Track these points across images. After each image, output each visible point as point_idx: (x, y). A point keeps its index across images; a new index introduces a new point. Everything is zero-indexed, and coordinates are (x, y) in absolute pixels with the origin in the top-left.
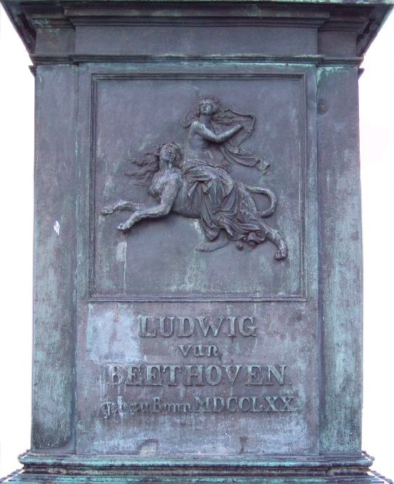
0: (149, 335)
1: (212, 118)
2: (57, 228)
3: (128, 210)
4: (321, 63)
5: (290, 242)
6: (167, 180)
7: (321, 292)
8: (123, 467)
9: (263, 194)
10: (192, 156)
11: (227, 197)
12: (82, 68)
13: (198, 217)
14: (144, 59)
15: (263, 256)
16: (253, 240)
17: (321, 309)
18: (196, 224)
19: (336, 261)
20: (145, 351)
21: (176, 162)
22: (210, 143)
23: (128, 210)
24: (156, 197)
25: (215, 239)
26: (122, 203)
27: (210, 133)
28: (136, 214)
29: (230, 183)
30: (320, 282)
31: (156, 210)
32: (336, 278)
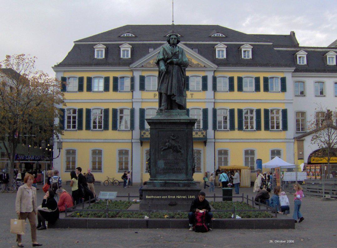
0: (165, 164)
1: (173, 136)
2: (154, 150)
3: (162, 148)
4: (187, 129)
5: (183, 152)
6: (167, 144)
7: (187, 158)
8: (162, 180)
9: (179, 146)
10: (171, 141)
11: (175, 146)
12: (157, 130)
13: (171, 149)
14: (165, 129)
15: (179, 154)
16: (178, 152)
17: (187, 160)
18: (171, 150)
19: (189, 154)
20: (165, 165)
21: (169, 142)
22: (173, 139)
23: (162, 148)
24: (166, 146)
25: (174, 151)
26: (162, 147)
27: (173, 138)
28: (164, 148)
29: (175, 145)
30: (187, 157)
31: (166, 148)
32: (189, 156)
